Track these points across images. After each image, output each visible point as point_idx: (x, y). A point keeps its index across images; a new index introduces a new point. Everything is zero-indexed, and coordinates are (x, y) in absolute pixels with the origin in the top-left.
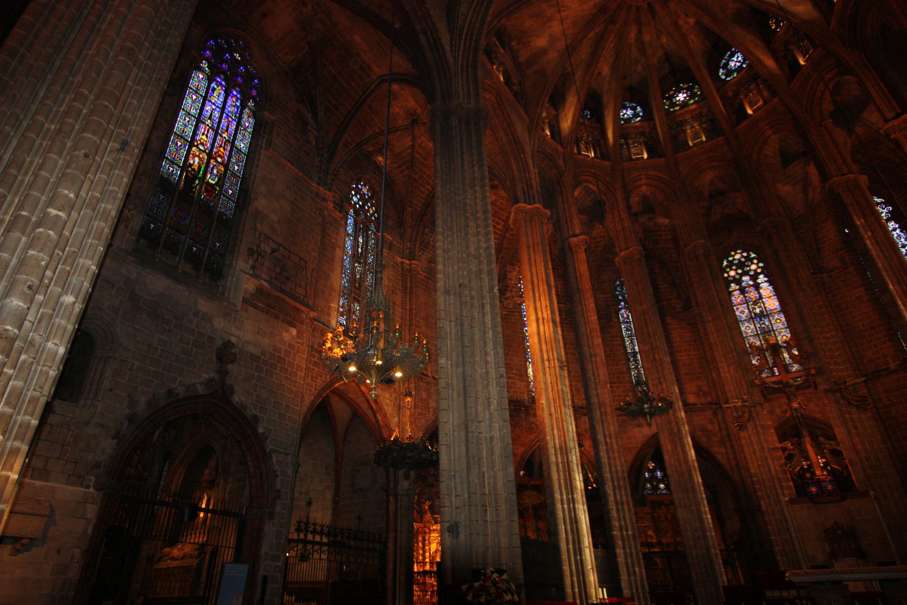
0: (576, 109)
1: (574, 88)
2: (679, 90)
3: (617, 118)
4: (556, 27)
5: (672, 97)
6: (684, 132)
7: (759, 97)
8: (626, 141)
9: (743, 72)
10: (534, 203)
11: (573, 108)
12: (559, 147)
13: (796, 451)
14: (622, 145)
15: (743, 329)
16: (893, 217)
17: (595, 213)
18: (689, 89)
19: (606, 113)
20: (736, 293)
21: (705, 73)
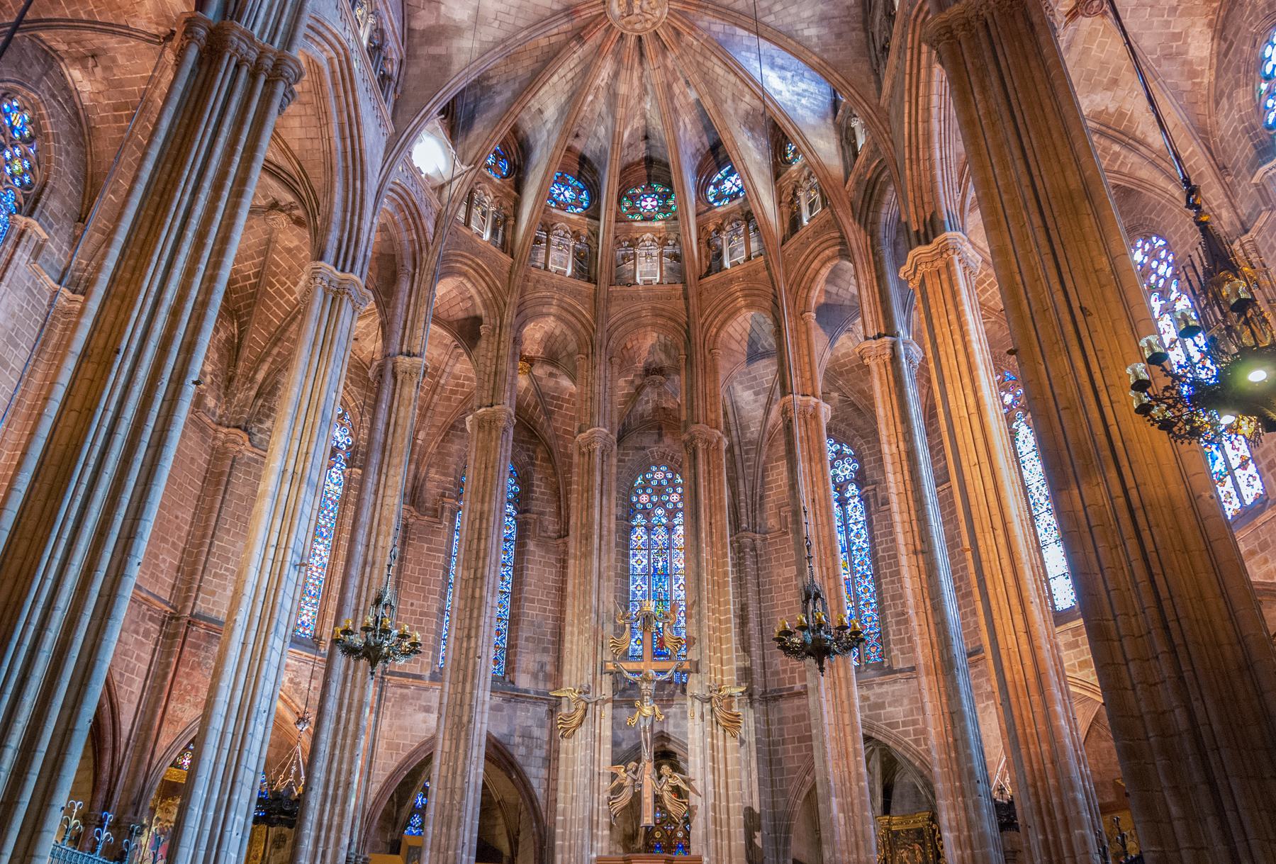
2: (650, 191)
5: (633, 198)
9: (736, 202)
13: (628, 782)
14: (537, 241)
15: (632, 588)
20: (640, 531)
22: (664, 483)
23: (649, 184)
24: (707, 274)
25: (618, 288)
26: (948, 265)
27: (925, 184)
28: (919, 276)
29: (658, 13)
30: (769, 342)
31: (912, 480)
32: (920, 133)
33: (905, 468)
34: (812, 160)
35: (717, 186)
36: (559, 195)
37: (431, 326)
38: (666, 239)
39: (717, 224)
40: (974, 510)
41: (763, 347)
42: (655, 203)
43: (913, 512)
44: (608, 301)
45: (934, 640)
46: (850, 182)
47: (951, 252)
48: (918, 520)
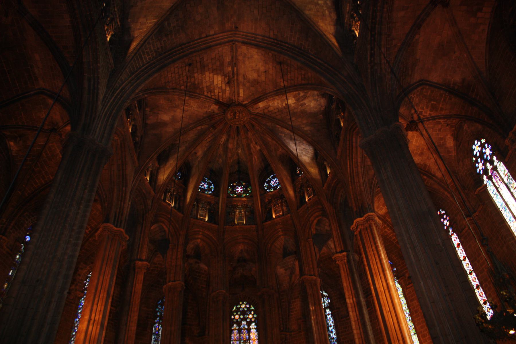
0: (172, 170)
1: (176, 156)
2: (239, 185)
3: (197, 187)
4: (179, 113)
5: (234, 187)
6: (235, 212)
7: (280, 209)
8: (197, 203)
9: (276, 191)
10: (120, 227)
11: (170, 169)
12: (153, 193)
14: (194, 206)
16: (330, 307)
17: (161, 246)
18: (245, 187)
19: (191, 180)
20: (236, 332)
21: (257, 181)
22: (246, 309)
24: (266, 221)
25: (228, 227)
26: (370, 226)
28: (358, 230)
29: (245, 118)
32: (354, 172)
33: (357, 309)
36: (202, 186)
38: (247, 205)
39: (269, 200)
40: (390, 332)
43: (361, 329)
46: (325, 186)
47: (371, 221)
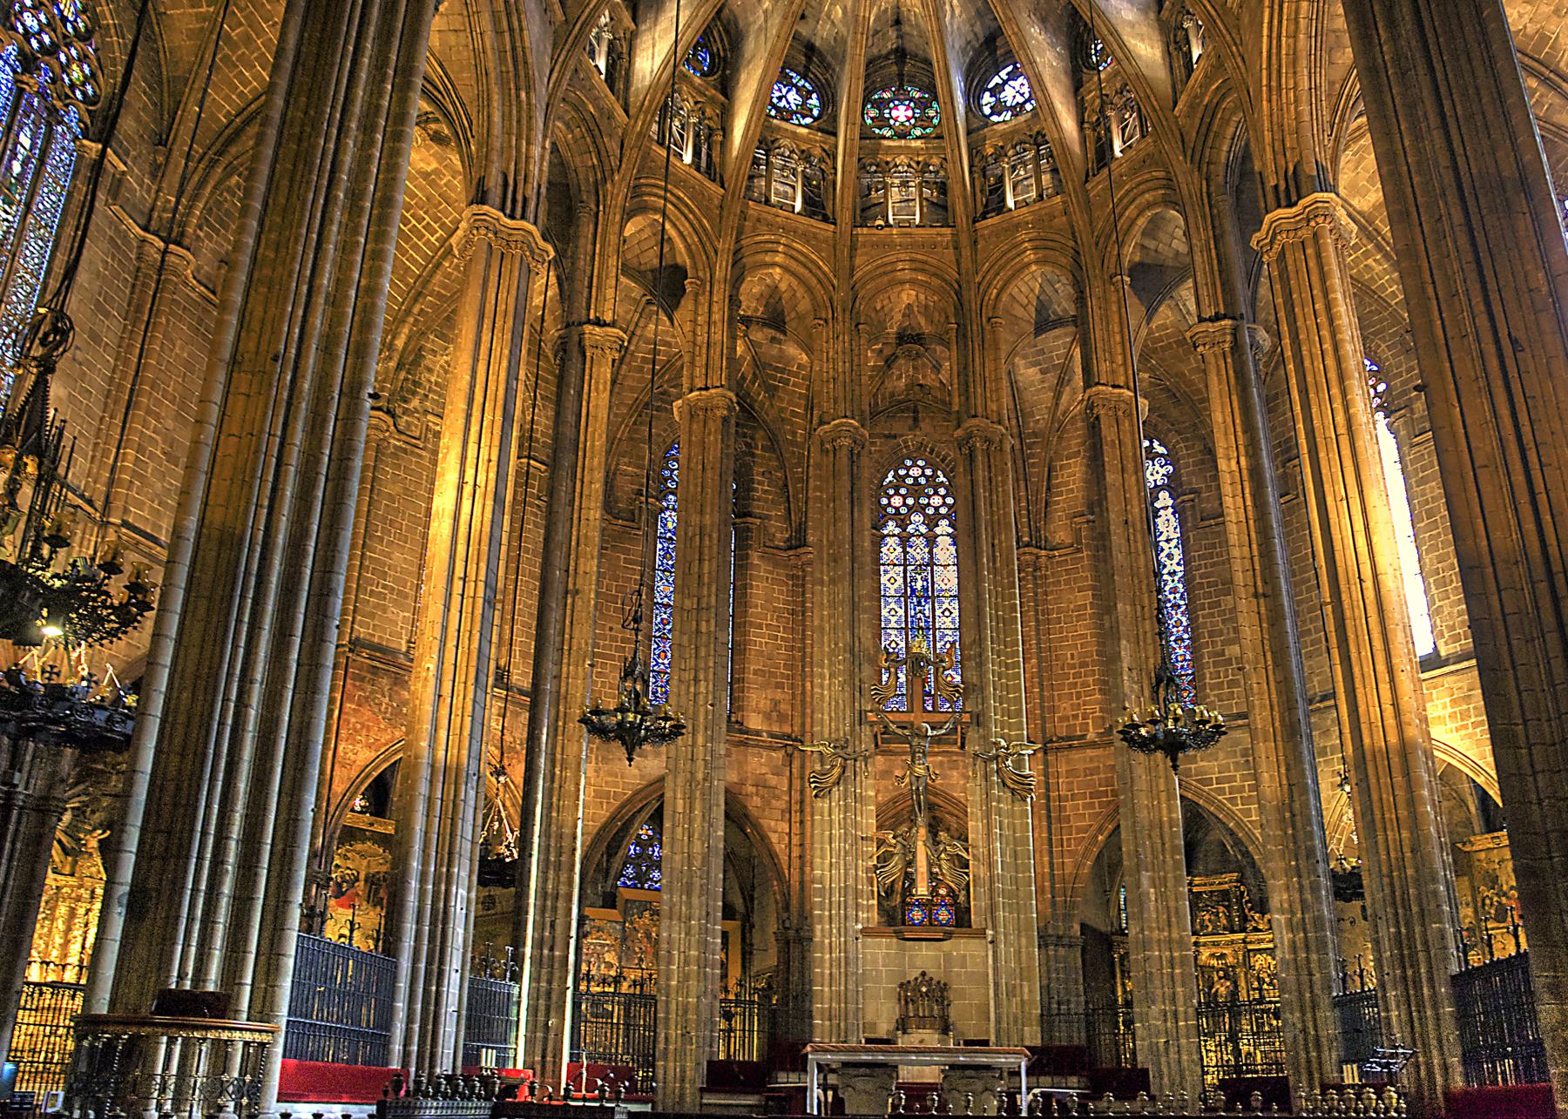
2: (901, 97)
5: (881, 105)
6: (886, 187)
7: (1033, 181)
9: (1022, 118)
18: (923, 105)
23: (901, 86)
25: (865, 230)
27: (1288, 121)
30: (1063, 303)
31: (1255, 505)
33: (1247, 491)
34: (1130, 70)
35: (993, 93)
37: (622, 279)
40: (1338, 556)
41: (1055, 313)
42: (910, 113)
43: (1254, 546)
44: (853, 248)
45: (1275, 701)
46: (1180, 105)
47: (1320, 220)
48: (1261, 556)
